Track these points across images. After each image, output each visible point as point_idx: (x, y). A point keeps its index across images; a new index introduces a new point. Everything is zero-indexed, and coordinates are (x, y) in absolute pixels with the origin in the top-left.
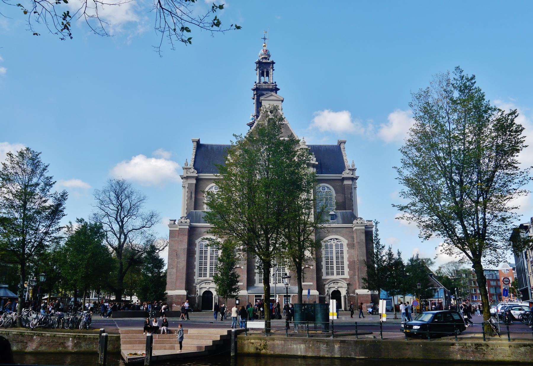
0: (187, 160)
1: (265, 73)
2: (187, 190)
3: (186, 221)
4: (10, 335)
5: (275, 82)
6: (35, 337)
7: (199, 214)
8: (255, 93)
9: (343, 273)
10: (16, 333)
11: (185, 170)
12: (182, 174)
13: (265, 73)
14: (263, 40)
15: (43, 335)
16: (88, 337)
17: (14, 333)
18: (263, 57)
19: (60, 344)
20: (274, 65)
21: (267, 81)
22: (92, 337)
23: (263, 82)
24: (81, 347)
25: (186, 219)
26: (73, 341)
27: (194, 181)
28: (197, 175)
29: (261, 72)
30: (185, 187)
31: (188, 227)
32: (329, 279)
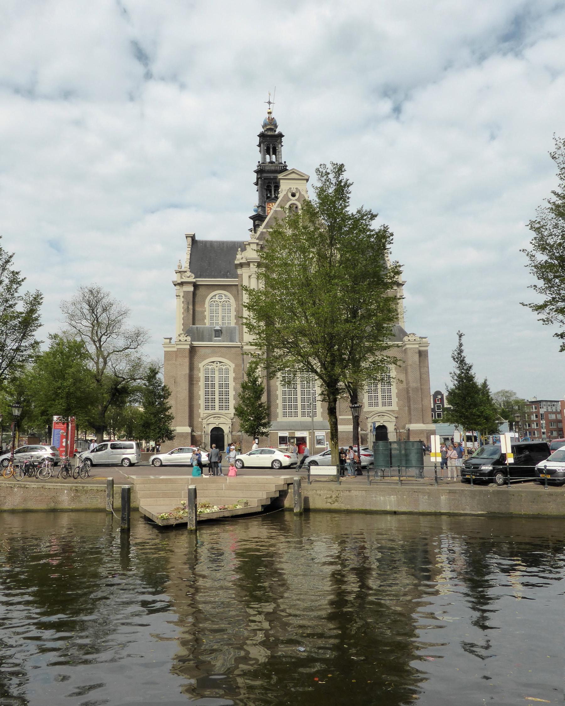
0: (180, 261)
1: (271, 150)
2: (182, 299)
3: (185, 338)
5: (285, 162)
6: (16, 490)
7: (201, 330)
8: (259, 176)
9: (390, 404)
11: (179, 274)
12: (175, 280)
13: (271, 150)
14: (268, 104)
15: (27, 486)
16: (89, 488)
18: (268, 127)
20: (282, 138)
21: (274, 160)
22: (95, 488)
23: (269, 162)
24: (80, 502)
25: (186, 336)
27: (191, 289)
28: (194, 280)
30: (180, 296)
31: (188, 347)
32: (372, 412)
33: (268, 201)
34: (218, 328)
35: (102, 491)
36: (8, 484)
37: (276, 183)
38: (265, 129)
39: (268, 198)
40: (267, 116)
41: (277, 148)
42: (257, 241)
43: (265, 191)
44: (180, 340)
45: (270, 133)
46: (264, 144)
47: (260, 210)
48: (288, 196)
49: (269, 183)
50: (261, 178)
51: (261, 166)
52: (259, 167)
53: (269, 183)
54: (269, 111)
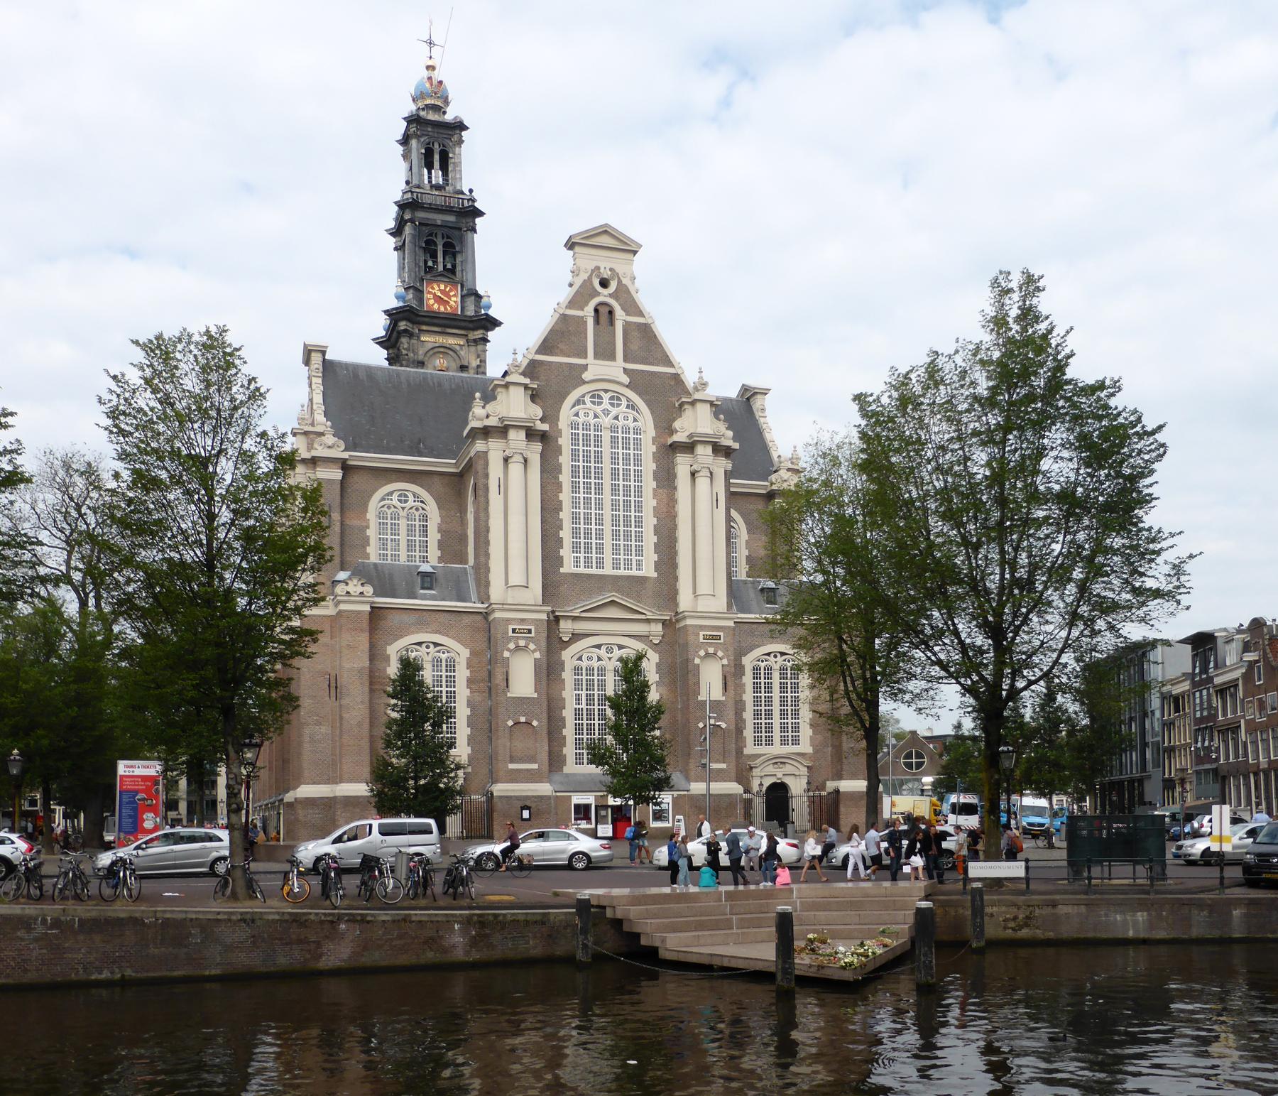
1: (436, 157)
3: (360, 589)
4: (258, 923)
5: (471, 191)
6: (343, 926)
8: (407, 217)
10: (277, 917)
13: (436, 157)
14: (426, 47)
15: (369, 918)
16: (509, 918)
17: (271, 917)
18: (428, 102)
19: (425, 943)
22: (521, 918)
26: (464, 932)
29: (423, 151)
33: (428, 276)
34: (425, 568)
35: (536, 922)
36: (325, 914)
37: (448, 237)
38: (421, 104)
39: (429, 270)
40: (426, 74)
41: (451, 155)
42: (527, 381)
43: (421, 253)
44: (348, 592)
45: (432, 116)
46: (419, 141)
47: (410, 296)
48: (591, 284)
49: (431, 235)
50: (412, 221)
51: (412, 192)
52: (409, 195)
53: (431, 235)
54: (430, 63)
